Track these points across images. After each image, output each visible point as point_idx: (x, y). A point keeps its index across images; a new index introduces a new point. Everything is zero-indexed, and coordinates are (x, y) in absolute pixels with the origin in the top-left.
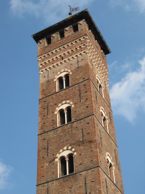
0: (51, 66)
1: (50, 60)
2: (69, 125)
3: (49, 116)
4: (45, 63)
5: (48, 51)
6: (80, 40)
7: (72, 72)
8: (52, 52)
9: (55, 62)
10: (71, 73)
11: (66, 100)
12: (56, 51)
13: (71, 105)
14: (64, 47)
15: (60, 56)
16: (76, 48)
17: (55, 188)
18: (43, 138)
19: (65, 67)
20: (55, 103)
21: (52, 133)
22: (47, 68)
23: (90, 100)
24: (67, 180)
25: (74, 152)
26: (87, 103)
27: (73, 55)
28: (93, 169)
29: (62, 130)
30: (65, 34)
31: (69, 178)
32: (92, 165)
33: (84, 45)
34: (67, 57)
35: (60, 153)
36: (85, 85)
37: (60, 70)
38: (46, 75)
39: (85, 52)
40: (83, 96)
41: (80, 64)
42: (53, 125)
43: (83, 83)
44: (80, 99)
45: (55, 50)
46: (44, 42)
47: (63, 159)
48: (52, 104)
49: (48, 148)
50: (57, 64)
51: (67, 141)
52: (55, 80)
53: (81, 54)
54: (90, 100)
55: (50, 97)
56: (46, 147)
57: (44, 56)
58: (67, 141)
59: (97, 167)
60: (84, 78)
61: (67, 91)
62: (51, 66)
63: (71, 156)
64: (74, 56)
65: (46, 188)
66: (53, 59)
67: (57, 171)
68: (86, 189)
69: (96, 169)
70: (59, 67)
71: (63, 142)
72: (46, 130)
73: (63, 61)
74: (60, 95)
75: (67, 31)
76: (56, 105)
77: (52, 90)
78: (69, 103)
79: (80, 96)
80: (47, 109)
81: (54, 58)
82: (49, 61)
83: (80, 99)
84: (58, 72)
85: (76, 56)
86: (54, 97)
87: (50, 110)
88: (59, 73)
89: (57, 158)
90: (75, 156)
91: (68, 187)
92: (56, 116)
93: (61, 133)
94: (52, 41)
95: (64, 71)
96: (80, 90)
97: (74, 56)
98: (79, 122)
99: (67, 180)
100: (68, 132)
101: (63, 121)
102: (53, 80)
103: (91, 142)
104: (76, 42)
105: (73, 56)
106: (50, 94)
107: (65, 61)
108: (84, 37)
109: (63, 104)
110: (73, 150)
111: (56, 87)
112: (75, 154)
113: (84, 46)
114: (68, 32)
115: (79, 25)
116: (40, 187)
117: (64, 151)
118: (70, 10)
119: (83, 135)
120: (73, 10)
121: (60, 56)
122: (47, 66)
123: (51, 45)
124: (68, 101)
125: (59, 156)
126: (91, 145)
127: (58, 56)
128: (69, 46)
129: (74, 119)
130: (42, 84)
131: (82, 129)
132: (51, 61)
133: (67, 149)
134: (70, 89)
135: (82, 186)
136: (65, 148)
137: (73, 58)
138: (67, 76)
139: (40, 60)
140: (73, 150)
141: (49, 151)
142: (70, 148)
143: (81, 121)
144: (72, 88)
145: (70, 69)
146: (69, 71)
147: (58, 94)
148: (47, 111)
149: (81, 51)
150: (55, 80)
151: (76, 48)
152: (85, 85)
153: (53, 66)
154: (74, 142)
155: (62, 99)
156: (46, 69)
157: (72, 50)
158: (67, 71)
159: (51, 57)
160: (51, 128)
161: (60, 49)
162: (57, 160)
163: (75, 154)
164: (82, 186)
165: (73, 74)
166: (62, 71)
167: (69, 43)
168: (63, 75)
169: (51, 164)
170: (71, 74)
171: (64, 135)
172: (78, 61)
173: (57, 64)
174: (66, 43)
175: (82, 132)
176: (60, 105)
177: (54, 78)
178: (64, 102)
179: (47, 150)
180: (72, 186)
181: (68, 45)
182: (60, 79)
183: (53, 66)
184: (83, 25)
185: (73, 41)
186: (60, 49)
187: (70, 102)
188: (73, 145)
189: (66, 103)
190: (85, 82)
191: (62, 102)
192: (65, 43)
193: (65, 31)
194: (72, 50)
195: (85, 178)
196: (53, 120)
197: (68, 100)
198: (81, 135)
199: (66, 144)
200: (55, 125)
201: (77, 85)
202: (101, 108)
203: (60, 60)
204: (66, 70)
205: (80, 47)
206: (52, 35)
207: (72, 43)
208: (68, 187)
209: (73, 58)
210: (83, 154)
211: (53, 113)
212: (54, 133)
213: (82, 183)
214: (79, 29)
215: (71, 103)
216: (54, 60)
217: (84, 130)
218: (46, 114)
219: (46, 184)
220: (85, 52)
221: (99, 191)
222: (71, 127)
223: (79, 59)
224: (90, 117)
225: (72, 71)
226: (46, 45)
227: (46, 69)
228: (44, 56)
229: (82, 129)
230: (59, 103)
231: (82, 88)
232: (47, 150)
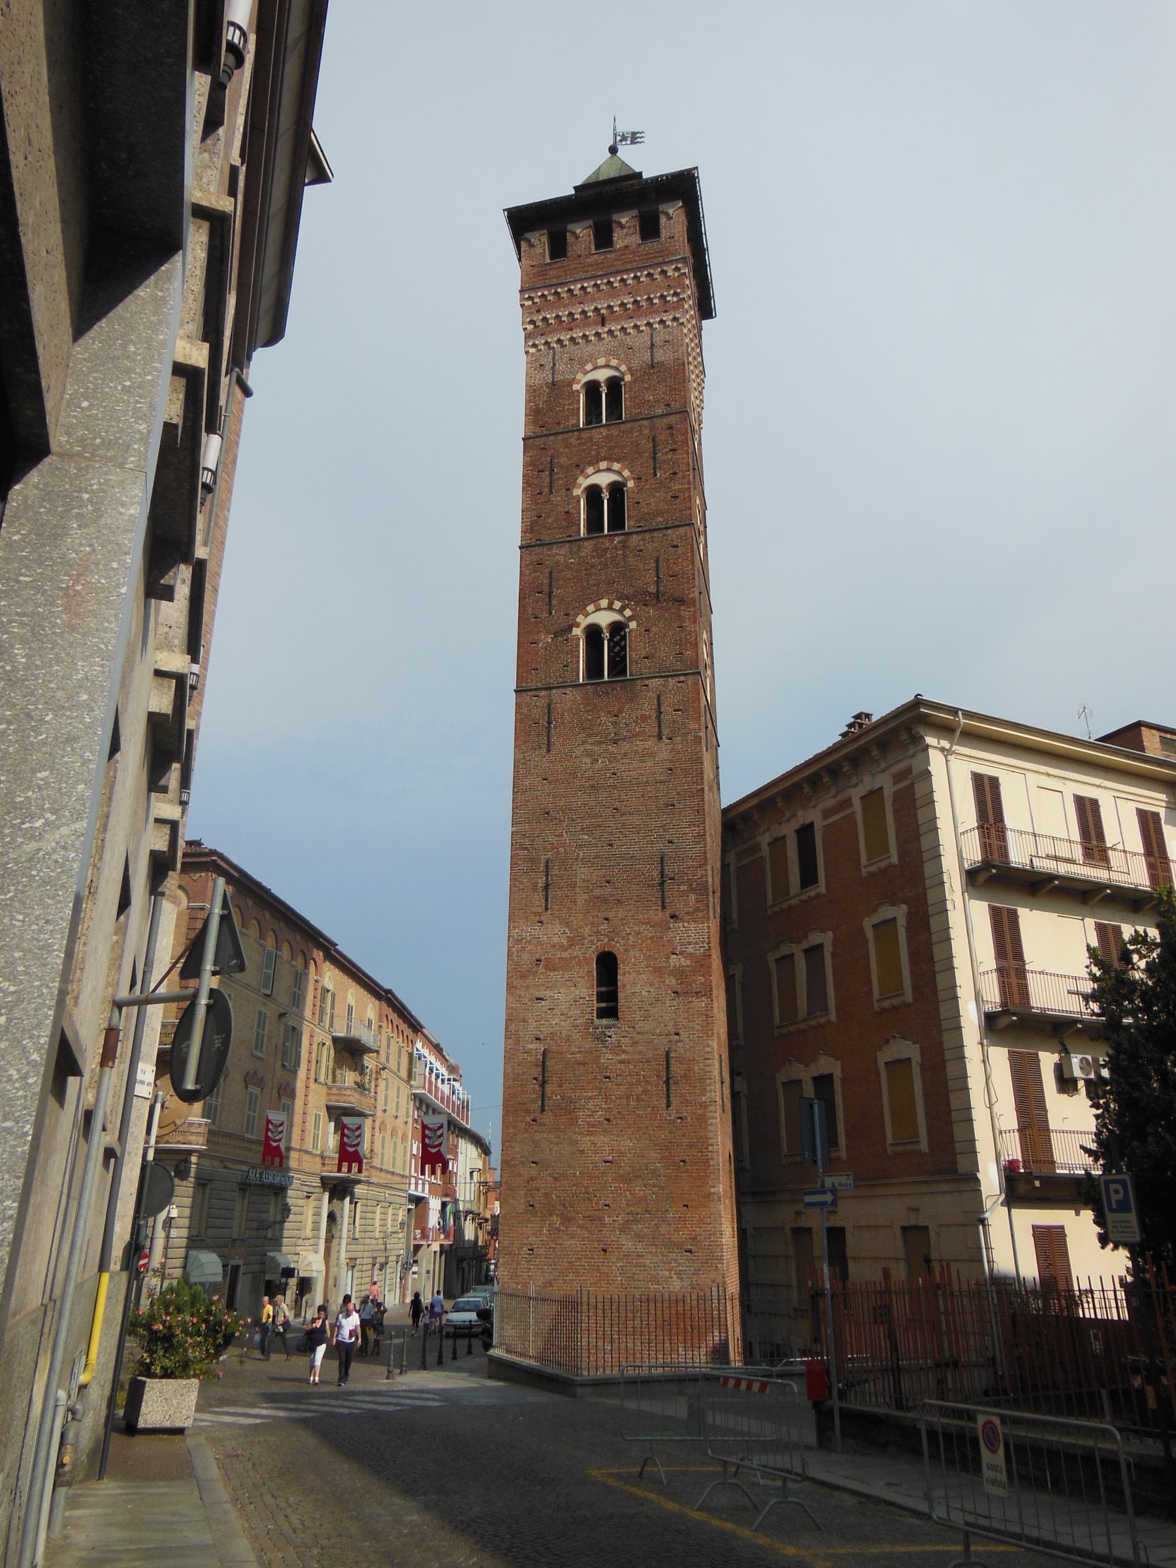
0: (565, 337)
1: (564, 313)
2: (617, 539)
3: (556, 498)
4: (545, 319)
5: (555, 281)
6: (663, 272)
7: (632, 375)
8: (570, 290)
9: (577, 326)
10: (628, 378)
12: (583, 288)
13: (626, 479)
14: (609, 283)
15: (596, 310)
16: (649, 299)
17: (571, 709)
18: (535, 558)
19: (611, 353)
20: (576, 460)
21: (563, 551)
22: (552, 339)
23: (683, 477)
24: (607, 693)
25: (631, 619)
26: (676, 487)
27: (639, 317)
28: (682, 678)
29: (595, 549)
30: (615, 234)
31: (613, 689)
32: (679, 665)
33: (676, 294)
34: (617, 320)
35: (587, 615)
36: (671, 428)
37: (592, 358)
38: (547, 360)
39: (675, 319)
40: (664, 462)
41: (660, 356)
42: (567, 527)
43: (665, 420)
44: (655, 469)
45: (579, 286)
46: (540, 240)
47: (593, 633)
48: (563, 461)
49: (551, 592)
50: (585, 337)
51: (611, 583)
52: (576, 387)
53: (662, 322)
54: (683, 477)
55: (560, 437)
56: (547, 589)
57: (543, 296)
58: (611, 583)
59: (693, 674)
60: (668, 405)
61: (614, 432)
62: (565, 337)
63: (617, 628)
64: (641, 323)
65: (542, 702)
66: (571, 314)
67: (578, 662)
68: (659, 727)
69: (690, 678)
70: (590, 348)
71: (597, 585)
72: (547, 540)
73: (606, 329)
74: (591, 438)
75: (622, 227)
76: (580, 467)
77: (567, 419)
78: (619, 473)
79: (654, 458)
80: (551, 475)
81: (577, 310)
82: (558, 317)
83: (655, 469)
84: (587, 361)
85: (649, 324)
86: (573, 441)
87: (559, 479)
88: (589, 367)
89: (578, 625)
90: (631, 631)
91: (609, 712)
92: (579, 501)
93: (593, 557)
95: (607, 366)
96: (654, 439)
97: (641, 323)
98: (647, 536)
99: (607, 693)
100: (613, 559)
101: (594, 524)
102: (570, 384)
103: (680, 601)
104: (649, 275)
105: (638, 323)
106: (560, 429)
107: (610, 332)
108: (680, 265)
109: (599, 471)
110: (628, 613)
111: (578, 409)
112: (633, 625)
113: (675, 299)
114: (625, 231)
115: (663, 220)
116: (526, 697)
117: (598, 609)
118: (615, 135)
119: (658, 578)
120: (624, 138)
121: (596, 310)
122: (550, 332)
123: (564, 262)
124: (616, 466)
125: (584, 621)
126: (679, 610)
127: (589, 308)
128: (626, 285)
129: (632, 523)
130: (535, 391)
131: (657, 561)
132: (564, 319)
133: (610, 608)
134: (623, 427)
135: (650, 717)
136: (604, 603)
137: (636, 327)
138: (614, 384)
139: (529, 307)
140: (628, 613)
141: (554, 602)
142: (617, 605)
143: (655, 534)
144: (629, 425)
145: (627, 361)
146: (623, 368)
147: (585, 435)
148: (548, 480)
149: (665, 311)
150: (576, 387)
151: (649, 299)
152: (671, 428)
153: (572, 339)
154: (631, 591)
155: (598, 453)
156: (547, 343)
157: (636, 302)
158: (616, 368)
159: (565, 306)
160: (560, 536)
161: (596, 285)
162: (577, 631)
164: (650, 717)
165: (634, 381)
166: (601, 361)
167: (627, 271)
168: (602, 375)
169: (560, 639)
170: (630, 382)
171: (600, 563)
172: (652, 345)
173: (585, 337)
174: (618, 272)
175: (657, 567)
176: (590, 470)
177: (574, 379)
178: (603, 465)
179: (550, 597)
180: (621, 711)
181: (622, 280)
182: (592, 388)
183: (572, 339)
184: (673, 216)
185: (641, 269)
186: (596, 285)
187: (623, 468)
188: (628, 598)
189: (609, 470)
190: (673, 419)
191: (598, 462)
192: (613, 269)
193: (614, 226)
194: (636, 302)
195: (659, 697)
196: (567, 512)
197: (618, 461)
198: (651, 577)
199: (607, 592)
200: (575, 528)
201: (645, 423)
203: (596, 324)
204: (614, 362)
205: (663, 297)
206: (570, 227)
207: (636, 277)
208: (609, 712)
209: (636, 327)
210: (654, 629)
211: (568, 490)
212: (571, 552)
213: (648, 709)
214: (664, 233)
215: (626, 473)
216: (574, 320)
217: (660, 563)
218: (546, 490)
219: (543, 693)
220: (675, 319)
221: (696, 737)
222: (624, 546)
223: (658, 339)
224: (682, 530)
225: (629, 369)
226: (548, 260)
227: (547, 343)
228: (543, 296)
229: (657, 561)
230: (590, 464)
231: (663, 436)
232: (550, 597)
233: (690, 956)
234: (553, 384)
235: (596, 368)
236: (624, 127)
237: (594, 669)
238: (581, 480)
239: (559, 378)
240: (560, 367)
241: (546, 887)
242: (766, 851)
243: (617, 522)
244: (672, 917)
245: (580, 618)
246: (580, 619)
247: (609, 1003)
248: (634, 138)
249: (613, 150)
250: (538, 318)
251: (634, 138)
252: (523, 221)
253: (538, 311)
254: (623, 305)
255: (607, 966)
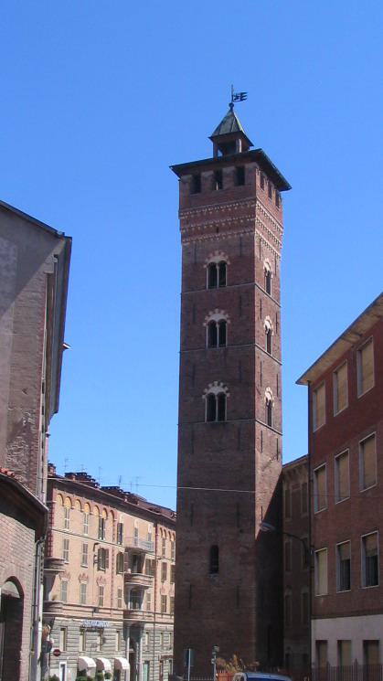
11: (221, 308)
34: (224, 229)
46: (188, 177)
76: (206, 312)
88: (211, 255)
94: (203, 187)
101: (213, 342)
120: (237, 97)
138: (222, 264)
140: (226, 389)
142: (222, 384)
163: (228, 395)
168: (217, 259)
172: (241, 245)
182: (212, 266)
197: (223, 308)
202: (268, 318)
215: (227, 316)
225: (230, 259)
233: (248, 548)
234: (196, 263)
235: (214, 255)
236: (237, 92)
237: (211, 417)
238: (207, 318)
239: (198, 260)
240: (198, 255)
241: (192, 516)
242: (301, 487)
243: (223, 341)
244: (241, 531)
245: (206, 390)
246: (206, 390)
247: (214, 567)
248: (241, 97)
249: (232, 105)
250: (187, 227)
251: (241, 97)
252: (179, 170)
253: (188, 223)
254: (226, 222)
255: (215, 552)
